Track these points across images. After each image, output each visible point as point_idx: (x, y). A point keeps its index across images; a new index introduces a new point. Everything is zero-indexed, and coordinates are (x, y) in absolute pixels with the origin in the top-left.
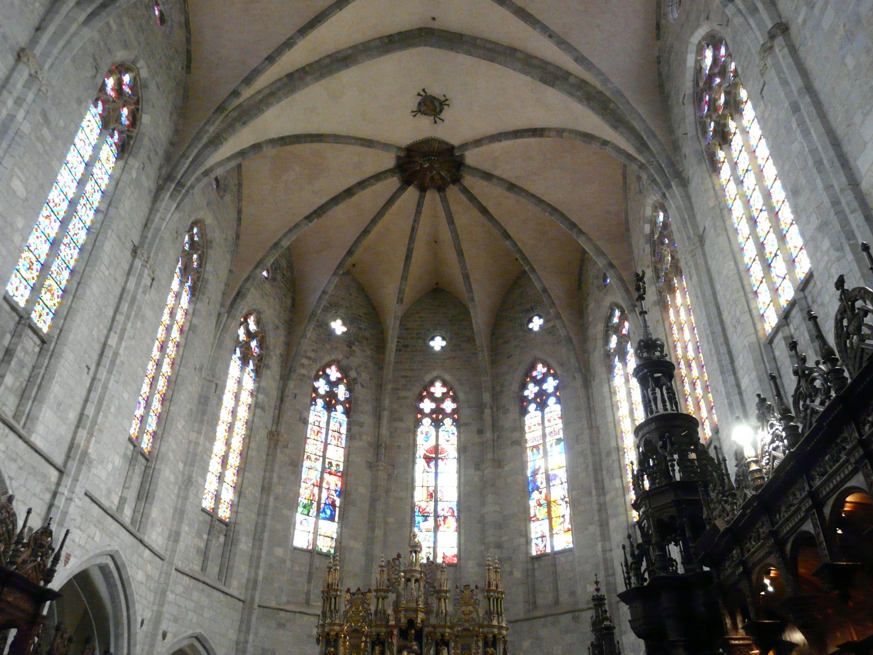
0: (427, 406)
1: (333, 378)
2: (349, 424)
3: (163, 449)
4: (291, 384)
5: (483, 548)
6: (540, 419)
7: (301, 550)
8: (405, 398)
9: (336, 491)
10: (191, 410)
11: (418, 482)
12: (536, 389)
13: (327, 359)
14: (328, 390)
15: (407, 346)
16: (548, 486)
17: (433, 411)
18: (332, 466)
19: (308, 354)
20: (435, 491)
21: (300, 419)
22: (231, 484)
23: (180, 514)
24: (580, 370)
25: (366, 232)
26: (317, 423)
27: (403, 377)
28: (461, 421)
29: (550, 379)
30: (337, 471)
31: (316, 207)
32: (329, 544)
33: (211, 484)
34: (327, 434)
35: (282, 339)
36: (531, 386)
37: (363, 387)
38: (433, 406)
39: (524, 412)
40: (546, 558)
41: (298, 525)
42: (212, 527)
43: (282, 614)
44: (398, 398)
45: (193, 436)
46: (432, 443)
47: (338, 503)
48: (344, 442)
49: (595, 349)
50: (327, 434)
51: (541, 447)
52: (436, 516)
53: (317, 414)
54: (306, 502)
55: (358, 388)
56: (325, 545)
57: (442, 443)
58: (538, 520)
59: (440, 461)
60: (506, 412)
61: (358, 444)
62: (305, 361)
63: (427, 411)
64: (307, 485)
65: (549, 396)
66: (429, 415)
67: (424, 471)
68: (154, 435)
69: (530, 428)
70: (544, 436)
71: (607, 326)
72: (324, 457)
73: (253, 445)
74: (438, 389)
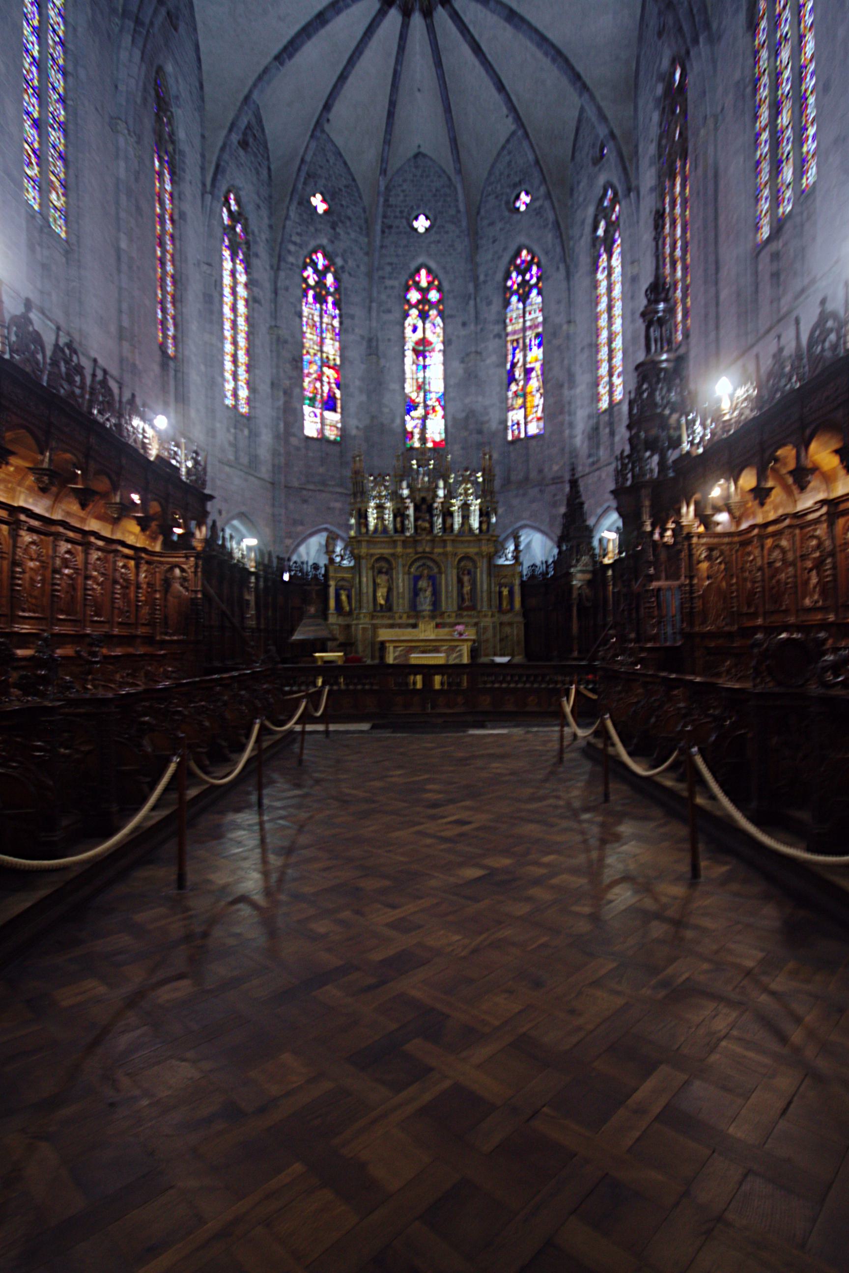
0: (414, 296)
1: (320, 267)
3: (187, 353)
4: (282, 274)
5: (466, 434)
6: (521, 312)
7: (312, 439)
8: (392, 287)
10: (200, 311)
11: (408, 375)
13: (312, 244)
15: (390, 227)
17: (419, 302)
20: (424, 383)
21: (296, 313)
23: (211, 412)
24: (565, 261)
25: (343, 78)
28: (446, 313)
31: (285, 41)
33: (229, 386)
35: (266, 221)
36: (514, 275)
37: (350, 274)
39: (507, 303)
42: (237, 421)
43: (304, 492)
44: (386, 288)
45: (207, 337)
46: (419, 335)
51: (521, 341)
52: (426, 406)
53: (309, 310)
54: (311, 395)
55: (345, 277)
56: (331, 434)
60: (489, 303)
61: (351, 337)
62: (292, 248)
65: (532, 287)
66: (416, 306)
67: (414, 363)
68: (174, 337)
70: (524, 329)
72: (322, 351)
73: (258, 342)
74: (423, 279)
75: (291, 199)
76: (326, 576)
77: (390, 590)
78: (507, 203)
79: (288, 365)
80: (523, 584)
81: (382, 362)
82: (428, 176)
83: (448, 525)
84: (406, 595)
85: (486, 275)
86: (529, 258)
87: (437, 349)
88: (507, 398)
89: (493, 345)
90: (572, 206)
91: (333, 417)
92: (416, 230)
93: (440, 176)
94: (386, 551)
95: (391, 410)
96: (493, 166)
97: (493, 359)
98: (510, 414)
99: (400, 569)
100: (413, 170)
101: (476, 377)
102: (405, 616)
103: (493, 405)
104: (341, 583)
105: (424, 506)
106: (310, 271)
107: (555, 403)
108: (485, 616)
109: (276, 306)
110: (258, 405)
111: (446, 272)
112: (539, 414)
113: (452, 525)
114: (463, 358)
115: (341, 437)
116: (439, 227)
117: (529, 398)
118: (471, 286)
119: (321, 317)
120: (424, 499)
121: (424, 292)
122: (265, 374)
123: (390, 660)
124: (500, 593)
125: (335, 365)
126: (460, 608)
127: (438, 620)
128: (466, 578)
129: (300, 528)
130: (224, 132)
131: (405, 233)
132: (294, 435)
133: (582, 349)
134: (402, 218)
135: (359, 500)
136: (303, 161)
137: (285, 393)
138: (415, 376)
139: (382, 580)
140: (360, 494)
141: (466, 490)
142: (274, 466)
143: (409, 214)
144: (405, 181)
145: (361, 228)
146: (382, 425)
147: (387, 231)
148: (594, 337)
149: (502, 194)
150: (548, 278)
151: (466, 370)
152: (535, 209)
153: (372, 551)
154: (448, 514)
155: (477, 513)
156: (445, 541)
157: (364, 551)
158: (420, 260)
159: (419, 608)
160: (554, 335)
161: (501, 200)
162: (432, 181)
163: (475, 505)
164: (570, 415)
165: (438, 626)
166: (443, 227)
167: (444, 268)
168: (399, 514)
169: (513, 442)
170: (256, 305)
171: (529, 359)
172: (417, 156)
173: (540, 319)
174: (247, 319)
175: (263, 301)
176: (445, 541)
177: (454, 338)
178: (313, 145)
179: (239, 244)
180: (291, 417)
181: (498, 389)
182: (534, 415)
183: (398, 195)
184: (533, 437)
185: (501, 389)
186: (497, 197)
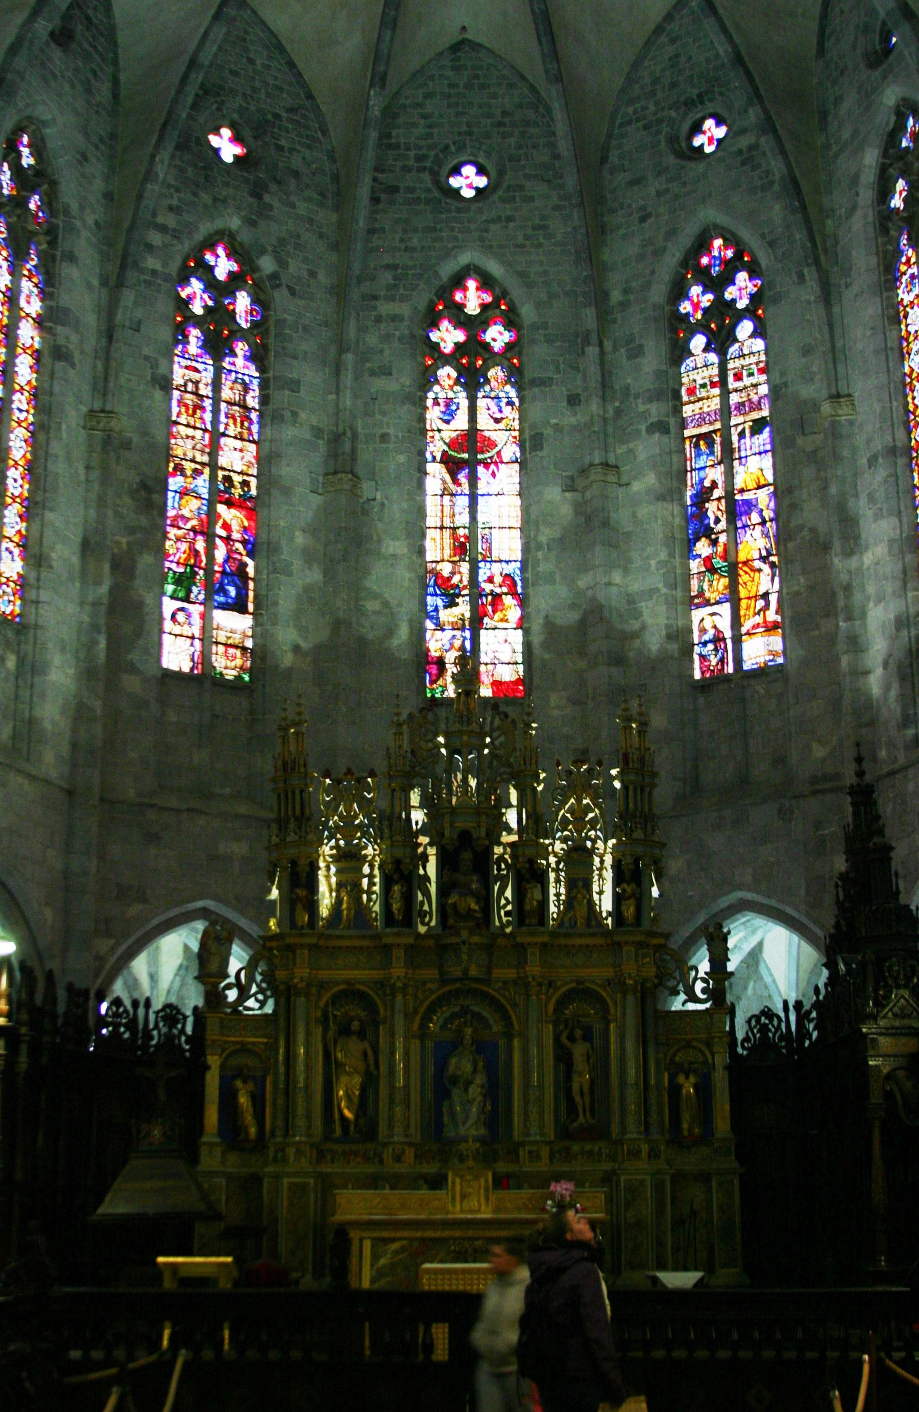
0: (448, 336)
1: (221, 273)
2: (264, 385)
4: (128, 297)
5: (582, 664)
6: (715, 371)
8: (395, 318)
9: (244, 542)
11: (432, 520)
12: (707, 300)
13: (205, 228)
14: (210, 303)
15: (394, 190)
16: (733, 529)
18: (232, 485)
19: (160, 220)
20: (472, 537)
22: (16, 539)
24: (817, 263)
26: (190, 387)
27: (388, 267)
28: (528, 375)
29: (742, 277)
30: (245, 497)
32: (239, 662)
34: (216, 412)
35: (99, 185)
36: (695, 290)
38: (459, 336)
40: (723, 687)
41: (168, 625)
43: (151, 815)
44: (378, 319)
46: (461, 422)
47: (251, 571)
48: (255, 428)
49: (854, 208)
50: (216, 412)
51: (718, 439)
53: (190, 366)
54: (181, 570)
55: (280, 297)
56: (227, 665)
57: (484, 422)
58: (707, 603)
59: (481, 469)
60: (636, 353)
61: (290, 432)
62: (156, 238)
63: (447, 348)
64: (180, 533)
69: (691, 391)
70: (725, 412)
71: (885, 154)
72: (214, 466)
73: (56, 448)
75: (161, 138)
76: (197, 1040)
77: (370, 1082)
78: (673, 140)
79: (128, 501)
80: (736, 1064)
81: (367, 489)
82: (483, 87)
83: (530, 905)
84: (415, 1097)
85: (626, 291)
86: (730, 254)
87: (506, 457)
88: (688, 576)
89: (646, 447)
90: (827, 147)
91: (234, 625)
92: (457, 191)
93: (511, 86)
94: (362, 975)
95: (386, 604)
96: (635, 66)
97: (646, 482)
98: (697, 615)
99: (400, 1022)
100: (450, 73)
101: (606, 524)
102: (410, 1154)
103: (653, 591)
104: (233, 1061)
105: (467, 852)
106: (196, 286)
107: (811, 588)
108: (635, 1154)
109: (107, 368)
110: (44, 596)
111: (529, 286)
112: (772, 616)
113: (544, 904)
114: (572, 478)
115: (251, 671)
116: (509, 188)
117: (744, 578)
118: (589, 316)
119: (216, 385)
120: (465, 836)
121: (473, 326)
122: (67, 522)
123: (365, 1277)
124: (675, 1090)
125: (245, 497)
126: (564, 1133)
127: (502, 1167)
128: (579, 1051)
129: (135, 910)
130: (19, 19)
131: (428, 202)
132: (133, 669)
133: (872, 461)
134: (421, 170)
135: (292, 837)
136: (193, 63)
137: (115, 566)
138: (447, 523)
139: (350, 1053)
140: (293, 825)
141: (579, 814)
142: (74, 746)
143: (439, 163)
144: (427, 96)
145: (322, 194)
146: (362, 642)
147: (383, 196)
148: (900, 434)
149: (659, 121)
150: (776, 300)
151: (579, 509)
152: (740, 152)
153: (324, 975)
154: (530, 875)
155: (608, 875)
156: (521, 949)
157: (302, 973)
158: (464, 259)
159: (450, 1132)
160: (802, 425)
161: (658, 132)
162: (494, 96)
163: (605, 852)
164: (849, 618)
165: (501, 1182)
166: (521, 188)
167: (522, 275)
168: (401, 874)
169: (705, 686)
170: (59, 365)
171: (739, 483)
172: (456, 47)
173: (764, 390)
174: (36, 395)
175: (77, 356)
176: (521, 949)
177: (548, 432)
178: (219, 33)
179: (33, 234)
180: (127, 623)
181: (663, 556)
182: (759, 619)
183: (414, 125)
184: (761, 672)
185: (672, 555)
186: (646, 128)
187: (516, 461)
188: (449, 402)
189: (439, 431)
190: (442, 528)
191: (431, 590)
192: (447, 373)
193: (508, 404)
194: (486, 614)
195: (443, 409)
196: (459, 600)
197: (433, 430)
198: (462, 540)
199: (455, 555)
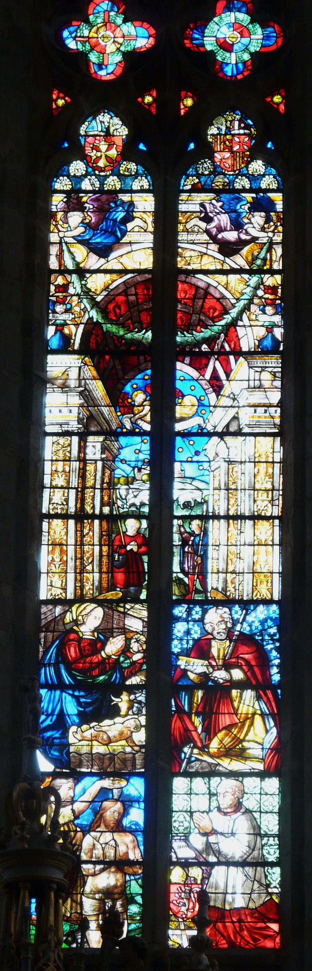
20: (157, 540)
57: (195, 253)
59: (183, 369)
87: (248, 338)
138: (95, 502)
187: (273, 350)
188: (106, 200)
189: (81, 272)
190: (81, 516)
191: (47, 674)
192: (104, 131)
193: (255, 207)
194: (187, 738)
195: (93, 218)
196: (123, 702)
197: (63, 271)
198: (132, 546)
199: (112, 587)
